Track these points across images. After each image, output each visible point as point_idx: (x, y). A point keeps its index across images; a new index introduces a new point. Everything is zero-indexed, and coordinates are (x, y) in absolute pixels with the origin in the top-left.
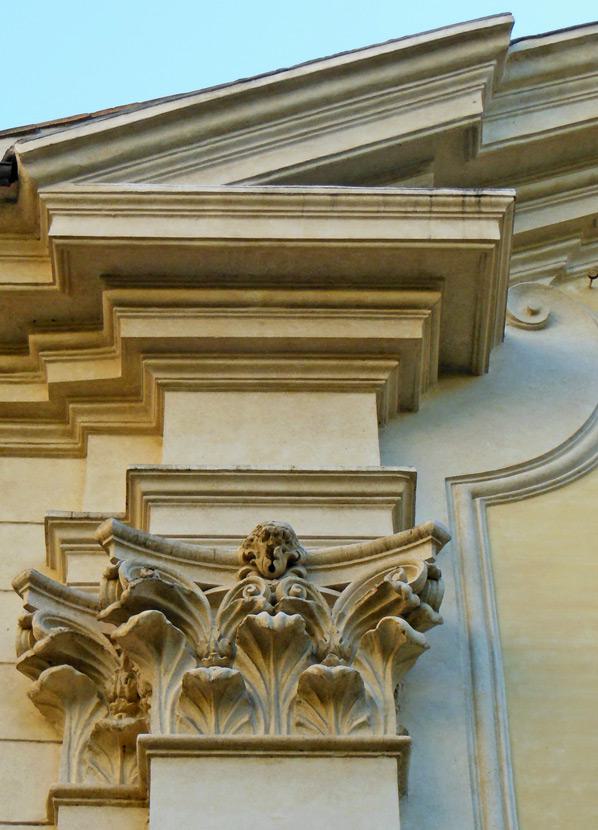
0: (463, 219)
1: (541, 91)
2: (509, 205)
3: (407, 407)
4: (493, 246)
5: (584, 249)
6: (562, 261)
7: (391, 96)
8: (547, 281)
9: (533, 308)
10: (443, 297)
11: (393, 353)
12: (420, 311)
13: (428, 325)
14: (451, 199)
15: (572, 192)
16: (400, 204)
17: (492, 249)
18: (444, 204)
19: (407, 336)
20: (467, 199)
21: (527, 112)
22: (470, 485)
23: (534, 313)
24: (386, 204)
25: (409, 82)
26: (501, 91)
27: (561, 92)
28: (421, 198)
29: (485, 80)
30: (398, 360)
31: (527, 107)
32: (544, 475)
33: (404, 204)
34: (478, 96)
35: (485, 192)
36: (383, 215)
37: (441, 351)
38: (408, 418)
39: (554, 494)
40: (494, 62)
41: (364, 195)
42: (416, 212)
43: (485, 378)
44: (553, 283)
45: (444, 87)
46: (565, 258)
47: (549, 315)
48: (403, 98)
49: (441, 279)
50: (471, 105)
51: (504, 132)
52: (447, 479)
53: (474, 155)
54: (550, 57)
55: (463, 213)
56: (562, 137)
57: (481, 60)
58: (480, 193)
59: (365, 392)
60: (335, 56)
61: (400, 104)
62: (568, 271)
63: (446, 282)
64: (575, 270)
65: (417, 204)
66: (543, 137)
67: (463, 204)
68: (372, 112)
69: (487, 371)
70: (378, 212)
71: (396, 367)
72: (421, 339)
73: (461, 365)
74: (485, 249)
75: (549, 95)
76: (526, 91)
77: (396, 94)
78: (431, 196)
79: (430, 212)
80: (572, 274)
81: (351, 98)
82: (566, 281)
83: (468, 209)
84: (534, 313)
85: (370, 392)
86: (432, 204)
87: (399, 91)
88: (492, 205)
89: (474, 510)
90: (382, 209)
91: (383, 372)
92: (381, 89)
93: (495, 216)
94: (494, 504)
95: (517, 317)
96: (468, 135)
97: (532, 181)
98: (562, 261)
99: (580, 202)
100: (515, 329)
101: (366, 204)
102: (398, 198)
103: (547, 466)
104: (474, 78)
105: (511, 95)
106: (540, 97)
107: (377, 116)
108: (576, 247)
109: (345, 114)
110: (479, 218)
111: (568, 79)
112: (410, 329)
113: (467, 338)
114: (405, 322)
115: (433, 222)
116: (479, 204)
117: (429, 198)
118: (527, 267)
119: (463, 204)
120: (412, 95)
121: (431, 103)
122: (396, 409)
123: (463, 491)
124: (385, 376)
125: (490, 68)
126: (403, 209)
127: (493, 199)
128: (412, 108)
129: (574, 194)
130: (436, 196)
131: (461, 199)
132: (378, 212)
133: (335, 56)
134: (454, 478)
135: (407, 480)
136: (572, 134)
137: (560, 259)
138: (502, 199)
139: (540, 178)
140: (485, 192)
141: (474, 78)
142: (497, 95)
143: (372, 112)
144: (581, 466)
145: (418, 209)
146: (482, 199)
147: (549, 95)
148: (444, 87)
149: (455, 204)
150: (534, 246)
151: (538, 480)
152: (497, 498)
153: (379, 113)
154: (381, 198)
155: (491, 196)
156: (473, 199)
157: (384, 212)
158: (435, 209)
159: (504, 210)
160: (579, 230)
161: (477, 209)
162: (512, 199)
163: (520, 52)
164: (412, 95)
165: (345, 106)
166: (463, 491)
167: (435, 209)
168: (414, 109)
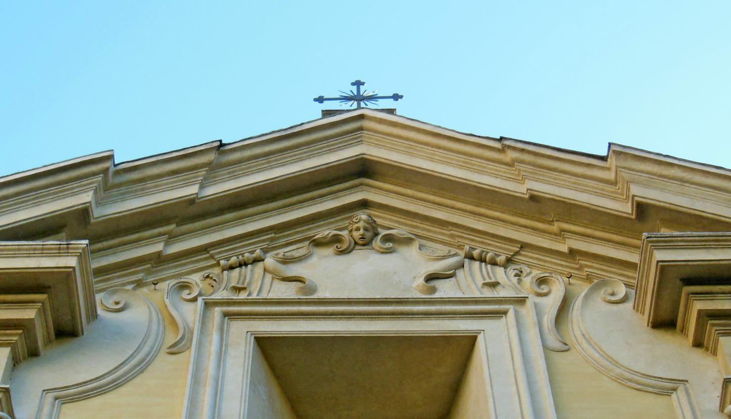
0: (59, 256)
1: (132, 189)
2: (83, 249)
3: (34, 353)
4: (71, 270)
5: (154, 269)
6: (140, 276)
7: (42, 194)
8: (130, 287)
9: (116, 301)
10: (48, 296)
11: (21, 326)
12: (36, 304)
13: (42, 311)
14: (54, 246)
15: (148, 240)
16: (27, 250)
17: (71, 272)
18: (50, 249)
19: (27, 317)
20: (62, 246)
21: (123, 200)
22: (55, 393)
23: (117, 303)
24: (19, 250)
25: (52, 187)
26: (109, 190)
27: (143, 189)
28: (38, 246)
29: (95, 185)
30: (22, 329)
31: (123, 197)
32: (84, 390)
33: (29, 250)
34: (91, 193)
35: (72, 242)
36: (18, 255)
37: (54, 322)
38: (35, 359)
39: (100, 397)
40: (102, 175)
41: (9, 245)
42: (35, 254)
43: (81, 338)
44: (134, 289)
45: (73, 188)
46: (142, 274)
47: (124, 304)
48: (48, 195)
49: (49, 287)
50: (86, 197)
51: (100, 213)
52: (44, 391)
53: (89, 223)
54: (137, 172)
55: (59, 253)
56: (141, 212)
57: (94, 174)
58: (69, 243)
59: (5, 347)
60: (12, 175)
61: (48, 198)
62: (144, 281)
63: (52, 289)
64: (148, 281)
65: (35, 249)
66: (128, 213)
67: (60, 249)
68: (30, 203)
69: (83, 334)
70: (15, 254)
71: (21, 333)
72: (34, 319)
73: (66, 332)
74: (67, 272)
75: (136, 191)
76: (123, 189)
77: (44, 193)
78: (43, 245)
79: (42, 253)
80: (146, 283)
81: (19, 196)
82: (142, 287)
83: (62, 251)
84: (117, 303)
85: (8, 347)
86: (43, 249)
87: (47, 191)
88: (74, 249)
89: (53, 406)
90: (17, 252)
91: (15, 336)
92: (37, 191)
93: (76, 254)
94: (66, 403)
95: (107, 306)
96: (84, 213)
97: (127, 235)
98: (140, 276)
99: (152, 246)
100: (106, 312)
101: (9, 250)
102: (26, 247)
103: (86, 386)
104: (90, 184)
105: (114, 192)
106: (132, 192)
107: (34, 205)
108: (149, 268)
109: (15, 204)
110: (67, 256)
111: (147, 183)
112: (29, 314)
113: (69, 318)
114: (27, 310)
115: (43, 258)
116: (68, 248)
117: (42, 246)
118: (120, 280)
119: (60, 249)
120: (54, 193)
121: (65, 197)
122: (27, 355)
123: (50, 397)
124: (15, 338)
125: (99, 178)
126: (28, 252)
127: (75, 246)
128: (54, 200)
129: (149, 242)
130: (46, 245)
131: (58, 246)
132: (15, 254)
133: (12, 175)
134: (48, 390)
135: (4, 392)
136: (146, 211)
137: (140, 275)
138: (80, 246)
139: (131, 234)
140: (72, 242)
141: (90, 184)
142: (105, 192)
143: (30, 203)
144: (117, 382)
145: (36, 252)
146: (70, 246)
147: (136, 191)
148: (73, 188)
149: (55, 249)
150: (125, 268)
151: (92, 390)
152: (68, 400)
153: (35, 203)
154: (17, 247)
155: (74, 244)
156: (65, 246)
157: (18, 254)
158: (44, 252)
159: (81, 251)
160: (151, 260)
161: (67, 251)
162: (86, 245)
163: (120, 169)
164: (54, 193)
165: (16, 200)
166: (50, 397)
167: (44, 252)
168: (55, 200)
